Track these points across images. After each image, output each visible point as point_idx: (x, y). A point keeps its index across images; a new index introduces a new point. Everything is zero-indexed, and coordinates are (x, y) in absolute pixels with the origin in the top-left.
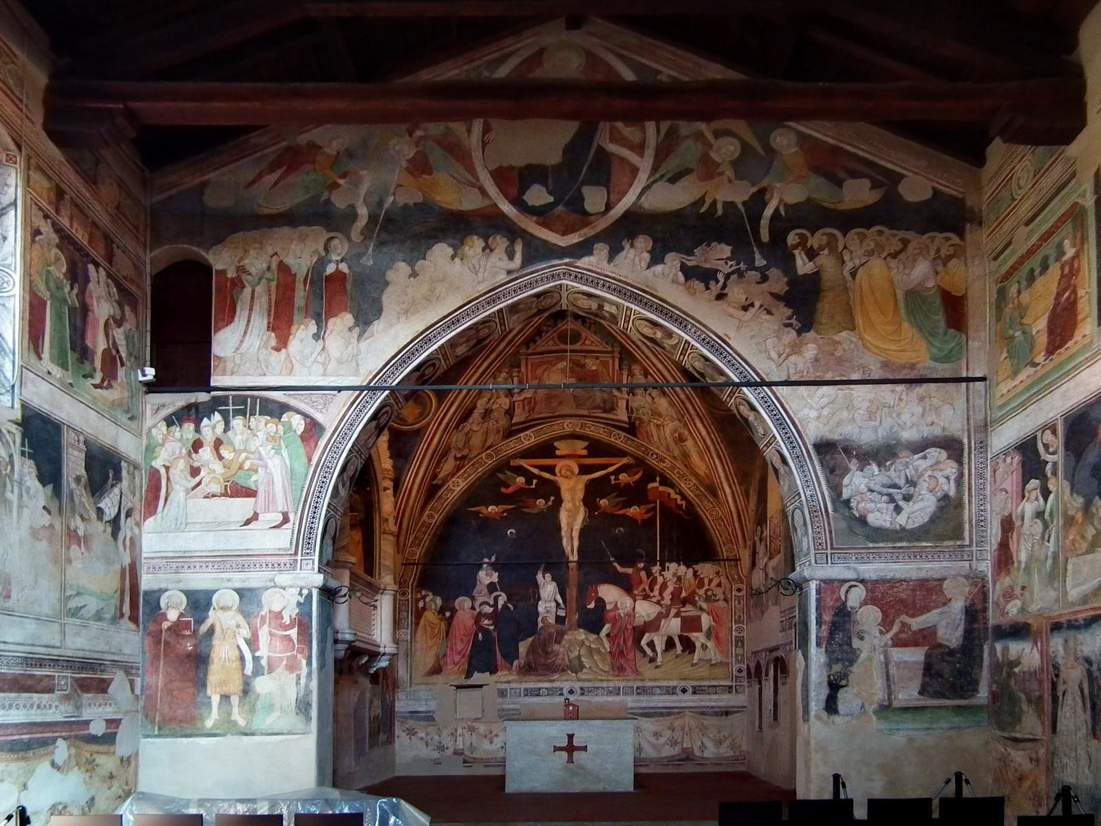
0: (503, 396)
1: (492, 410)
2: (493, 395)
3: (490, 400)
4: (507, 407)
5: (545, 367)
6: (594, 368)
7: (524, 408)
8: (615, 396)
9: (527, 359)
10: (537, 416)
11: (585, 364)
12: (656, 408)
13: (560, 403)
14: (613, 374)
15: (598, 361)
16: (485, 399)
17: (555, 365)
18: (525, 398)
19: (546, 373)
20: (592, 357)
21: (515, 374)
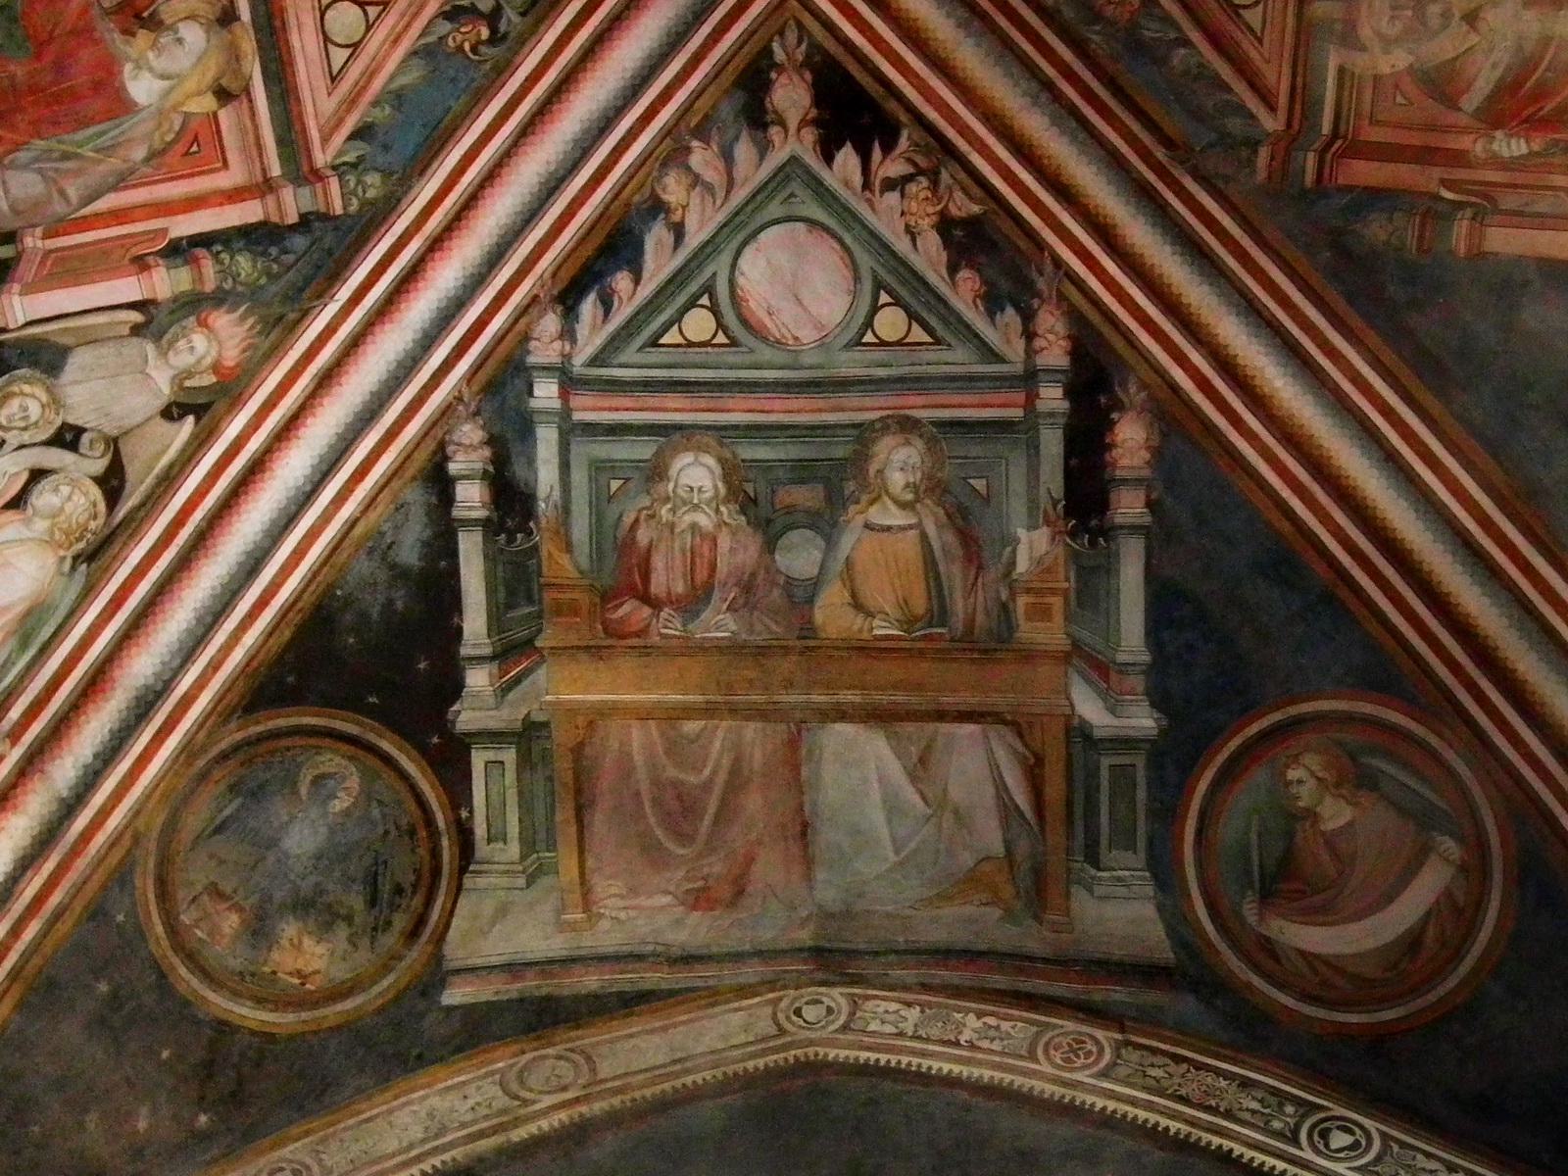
6: (142, 88)
11: (154, 24)
14: (119, 216)
15: (208, 103)
20: (234, 55)
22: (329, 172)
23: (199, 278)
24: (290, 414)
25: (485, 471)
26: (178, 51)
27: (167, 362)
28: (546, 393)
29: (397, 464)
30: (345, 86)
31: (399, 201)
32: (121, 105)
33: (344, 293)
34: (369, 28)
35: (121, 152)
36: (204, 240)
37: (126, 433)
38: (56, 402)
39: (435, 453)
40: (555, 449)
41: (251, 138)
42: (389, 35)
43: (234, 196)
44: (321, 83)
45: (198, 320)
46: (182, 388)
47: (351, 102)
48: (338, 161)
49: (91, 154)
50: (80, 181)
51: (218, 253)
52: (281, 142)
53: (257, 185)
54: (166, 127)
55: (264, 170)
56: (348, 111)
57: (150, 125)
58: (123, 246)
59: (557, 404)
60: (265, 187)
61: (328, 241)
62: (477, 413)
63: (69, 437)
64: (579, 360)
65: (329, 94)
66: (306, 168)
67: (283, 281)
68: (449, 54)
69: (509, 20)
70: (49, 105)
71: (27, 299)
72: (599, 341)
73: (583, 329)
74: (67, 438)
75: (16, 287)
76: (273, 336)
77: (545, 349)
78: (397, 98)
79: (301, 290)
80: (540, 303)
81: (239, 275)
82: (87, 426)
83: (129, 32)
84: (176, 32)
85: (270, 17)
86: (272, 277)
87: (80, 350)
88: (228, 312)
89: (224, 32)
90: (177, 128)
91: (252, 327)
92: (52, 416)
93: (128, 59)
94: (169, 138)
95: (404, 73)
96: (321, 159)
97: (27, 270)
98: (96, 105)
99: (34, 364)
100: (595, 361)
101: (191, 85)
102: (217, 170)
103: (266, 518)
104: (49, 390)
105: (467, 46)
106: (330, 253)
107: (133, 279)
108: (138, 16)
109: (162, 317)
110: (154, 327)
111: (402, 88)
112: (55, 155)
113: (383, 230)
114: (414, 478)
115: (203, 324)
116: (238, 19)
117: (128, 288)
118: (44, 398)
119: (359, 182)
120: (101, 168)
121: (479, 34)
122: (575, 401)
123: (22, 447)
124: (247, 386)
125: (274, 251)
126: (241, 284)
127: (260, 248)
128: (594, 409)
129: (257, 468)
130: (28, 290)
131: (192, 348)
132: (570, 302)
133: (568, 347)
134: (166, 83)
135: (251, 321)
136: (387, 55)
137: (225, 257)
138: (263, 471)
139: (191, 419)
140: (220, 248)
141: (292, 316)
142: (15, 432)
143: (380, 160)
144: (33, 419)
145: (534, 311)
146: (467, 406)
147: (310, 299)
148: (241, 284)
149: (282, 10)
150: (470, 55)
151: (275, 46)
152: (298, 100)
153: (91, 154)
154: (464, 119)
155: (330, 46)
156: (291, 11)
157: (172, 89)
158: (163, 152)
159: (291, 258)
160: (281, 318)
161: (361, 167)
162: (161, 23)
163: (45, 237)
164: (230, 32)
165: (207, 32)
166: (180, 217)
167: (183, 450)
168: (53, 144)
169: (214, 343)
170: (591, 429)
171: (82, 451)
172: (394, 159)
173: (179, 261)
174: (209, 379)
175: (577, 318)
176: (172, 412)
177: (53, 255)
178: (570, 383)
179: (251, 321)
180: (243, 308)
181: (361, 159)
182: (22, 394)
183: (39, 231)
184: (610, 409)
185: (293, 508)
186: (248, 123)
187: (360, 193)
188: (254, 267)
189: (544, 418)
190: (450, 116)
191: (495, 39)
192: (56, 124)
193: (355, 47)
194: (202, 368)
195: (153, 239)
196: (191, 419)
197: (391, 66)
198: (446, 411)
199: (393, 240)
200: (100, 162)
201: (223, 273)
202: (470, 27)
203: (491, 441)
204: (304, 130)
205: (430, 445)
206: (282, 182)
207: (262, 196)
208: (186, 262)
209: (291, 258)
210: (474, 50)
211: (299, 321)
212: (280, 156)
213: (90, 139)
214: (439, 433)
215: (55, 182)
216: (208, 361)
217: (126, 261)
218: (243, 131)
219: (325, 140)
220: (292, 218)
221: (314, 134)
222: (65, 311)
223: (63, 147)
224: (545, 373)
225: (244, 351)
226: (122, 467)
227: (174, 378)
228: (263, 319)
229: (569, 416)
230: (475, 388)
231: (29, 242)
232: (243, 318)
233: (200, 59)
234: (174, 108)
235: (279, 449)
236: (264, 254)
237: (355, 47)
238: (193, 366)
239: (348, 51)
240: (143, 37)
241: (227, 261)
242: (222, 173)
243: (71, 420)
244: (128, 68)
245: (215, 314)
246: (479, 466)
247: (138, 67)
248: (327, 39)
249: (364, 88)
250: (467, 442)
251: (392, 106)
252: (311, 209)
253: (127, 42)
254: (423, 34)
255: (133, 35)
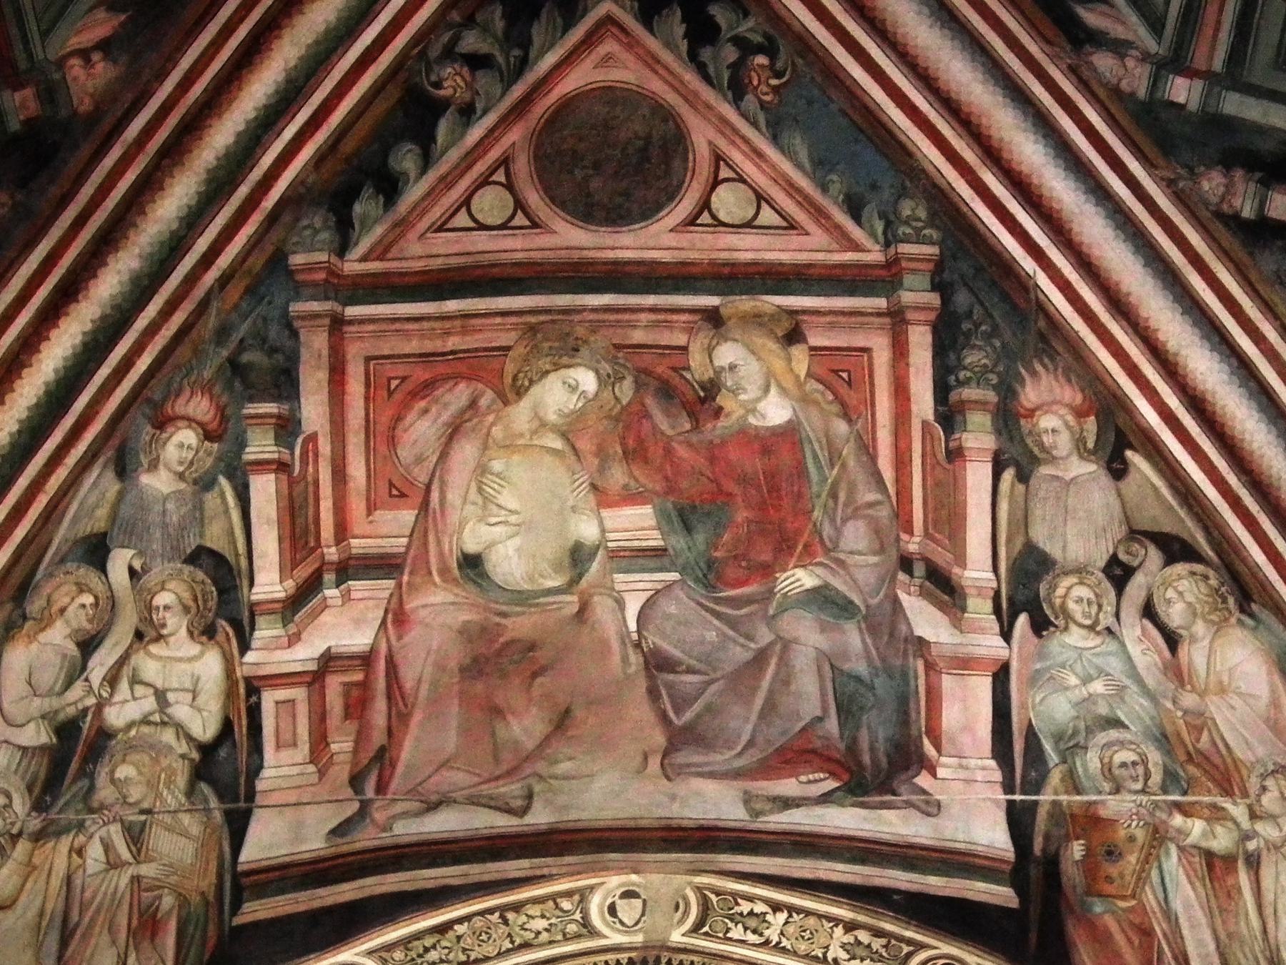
0: (176, 624)
1: (104, 735)
2: (109, 608)
3: (88, 645)
4: (204, 726)
5: (459, 395)
6: (775, 412)
7: (320, 741)
8: (922, 644)
9: (337, 324)
10: (410, 829)
11: (712, 388)
12: (1198, 722)
13: (562, 721)
15: (800, 356)
16: (58, 636)
17: (520, 392)
18: (329, 661)
19: (465, 452)
21: (261, 446)
22: (892, 251)
23: (981, 405)
24: (1149, 356)
25: (1260, 181)
26: (742, 371)
27: (1062, 458)
28: (1181, 90)
29: (1231, 266)
30: (800, 216)
31: (935, 186)
32: (789, 434)
33: (1028, 264)
34: (742, 180)
35: (838, 443)
36: (942, 391)
37: (1127, 518)
38: (1080, 571)
39: (1226, 225)
40: (1251, 101)
41: (842, 319)
42: (752, 160)
43: (900, 350)
44: (795, 240)
45: (1025, 417)
46: (1094, 452)
47: (819, 214)
48: (881, 238)
49: (835, 472)
50: (861, 487)
51: (957, 380)
52: (852, 293)
53: (894, 325)
54: (819, 397)
55: (879, 315)
56: (828, 217)
57: (814, 414)
58: (933, 468)
59: (1198, 85)
60: (897, 320)
61: (965, 266)
62: (1191, 170)
63: (1118, 572)
64: (1151, 45)
65: (807, 234)
66: (883, 273)
67: (1002, 325)
68: (780, 101)
69: (751, 30)
70: (780, 498)
71: (969, 565)
72: (1134, 18)
73: (1118, 31)
74: (1119, 574)
75: (956, 570)
76: (1060, 349)
77: (1136, 79)
78: (821, 167)
79: (1015, 307)
80: (1078, 66)
81: (985, 366)
82: (1111, 552)
83: (718, 412)
84: (723, 368)
85: (718, 277)
86: (995, 332)
87: (1032, 533)
88: (1023, 386)
89: (730, 323)
90: (821, 387)
91: (1045, 366)
92: (1093, 578)
93: (744, 417)
94: (831, 397)
95: (796, 153)
96: (874, 255)
97: (942, 557)
98: (785, 459)
99: (1038, 578)
100: (1156, 25)
101: (778, 365)
102: (870, 359)
103: (1256, 415)
104: (1066, 574)
105: (774, 82)
106: (979, 270)
107: (968, 464)
108: (703, 401)
109: (1014, 451)
110: (1024, 461)
111: (811, 160)
112: (831, 503)
113: (965, 209)
114: (1251, 254)
115: (1031, 413)
116: (716, 310)
117: (978, 476)
118: (1072, 580)
119: (907, 223)
120: (851, 463)
121: (761, 66)
122: (1200, 63)
123: (1117, 616)
124: (1106, 387)
125: (966, 326)
126: (995, 365)
127: (961, 339)
128: (1213, 48)
129: (1198, 404)
130: (961, 560)
131: (1053, 431)
132: (1082, 36)
133: (1134, 53)
134: (773, 390)
135: (1039, 367)
136: (773, 166)
137: (962, 375)
138: (1204, 400)
139: (1129, 454)
140: (953, 378)
141: (1042, 323)
142: (1101, 616)
143: (887, 194)
144: (1092, 596)
145: (1086, 74)
146: (1180, 177)
147: (1028, 301)
148: (995, 365)
149: (712, 263)
150: (784, 80)
151: (749, 277)
152: (809, 266)
153: (835, 472)
154: (857, 98)
155: (757, 223)
156: (714, 255)
157: (780, 386)
158: (843, 405)
159: (978, 312)
160: (1042, 337)
161: (892, 218)
162: (711, 381)
163: (911, 533)
164: (730, 318)
165: (726, 340)
166: (914, 408)
167: (1161, 472)
168: (819, 504)
169: (1055, 408)
170: (1237, 55)
171: (1135, 564)
172: (888, 182)
173: (959, 418)
174: (1091, 424)
175: (1103, 34)
176: (1118, 469)
177: (931, 531)
178: (1176, 62)
179: (1039, 367)
180: (1023, 371)
181: (883, 215)
182: (1065, 596)
183: (904, 537)
184: (1217, 30)
185: (1252, 384)
186: (828, 319)
187: (920, 224)
188: (980, 348)
189: (1212, 102)
190: (850, 112)
191: (769, 49)
192: (799, 496)
193: (761, 198)
194: (1077, 428)
195: (932, 438)
196: (1129, 454)
197: (786, 166)
198: (1180, 199)
199: (977, 199)
200: (844, 466)
201: (980, 378)
202: (753, 74)
203: (1228, 162)
204: (842, 266)
205: (1218, 228)
206: (894, 299)
207: (907, 322)
208: (962, 412)
209: (978, 312)
210: (778, 75)
211: (1048, 316)
212: (866, 295)
213: (819, 468)
214: (1205, 214)
215: (857, 509)
216: (1070, 418)
217: (948, 466)
218: (832, 326)
219: (857, 247)
220: (934, 299)
221: (849, 256)
222: (989, 536)
223: (824, 495)
224: (1160, 85)
225: (1069, 381)
226: (1166, 535)
227: (1081, 457)
228: (1038, 355)
229: (1216, 75)
230: (1161, 162)
231: (913, 548)
232: (1034, 374)
233: (753, 353)
234: (800, 385)
235: (1185, 377)
236: (968, 335)
237: (761, 198)
238: (1072, 433)
239: (764, 204)
240: (723, 400)
241: (969, 374)
242: (875, 355)
243: (1102, 564)
244: (752, 420)
245: (1022, 397)
246: (1252, 186)
247: (753, 411)
248: (749, 225)
249: (807, 197)
250: (1222, 189)
251: (831, 171)
252: (928, 279)
253: (728, 415)
254: (755, 124)
255: (721, 409)
